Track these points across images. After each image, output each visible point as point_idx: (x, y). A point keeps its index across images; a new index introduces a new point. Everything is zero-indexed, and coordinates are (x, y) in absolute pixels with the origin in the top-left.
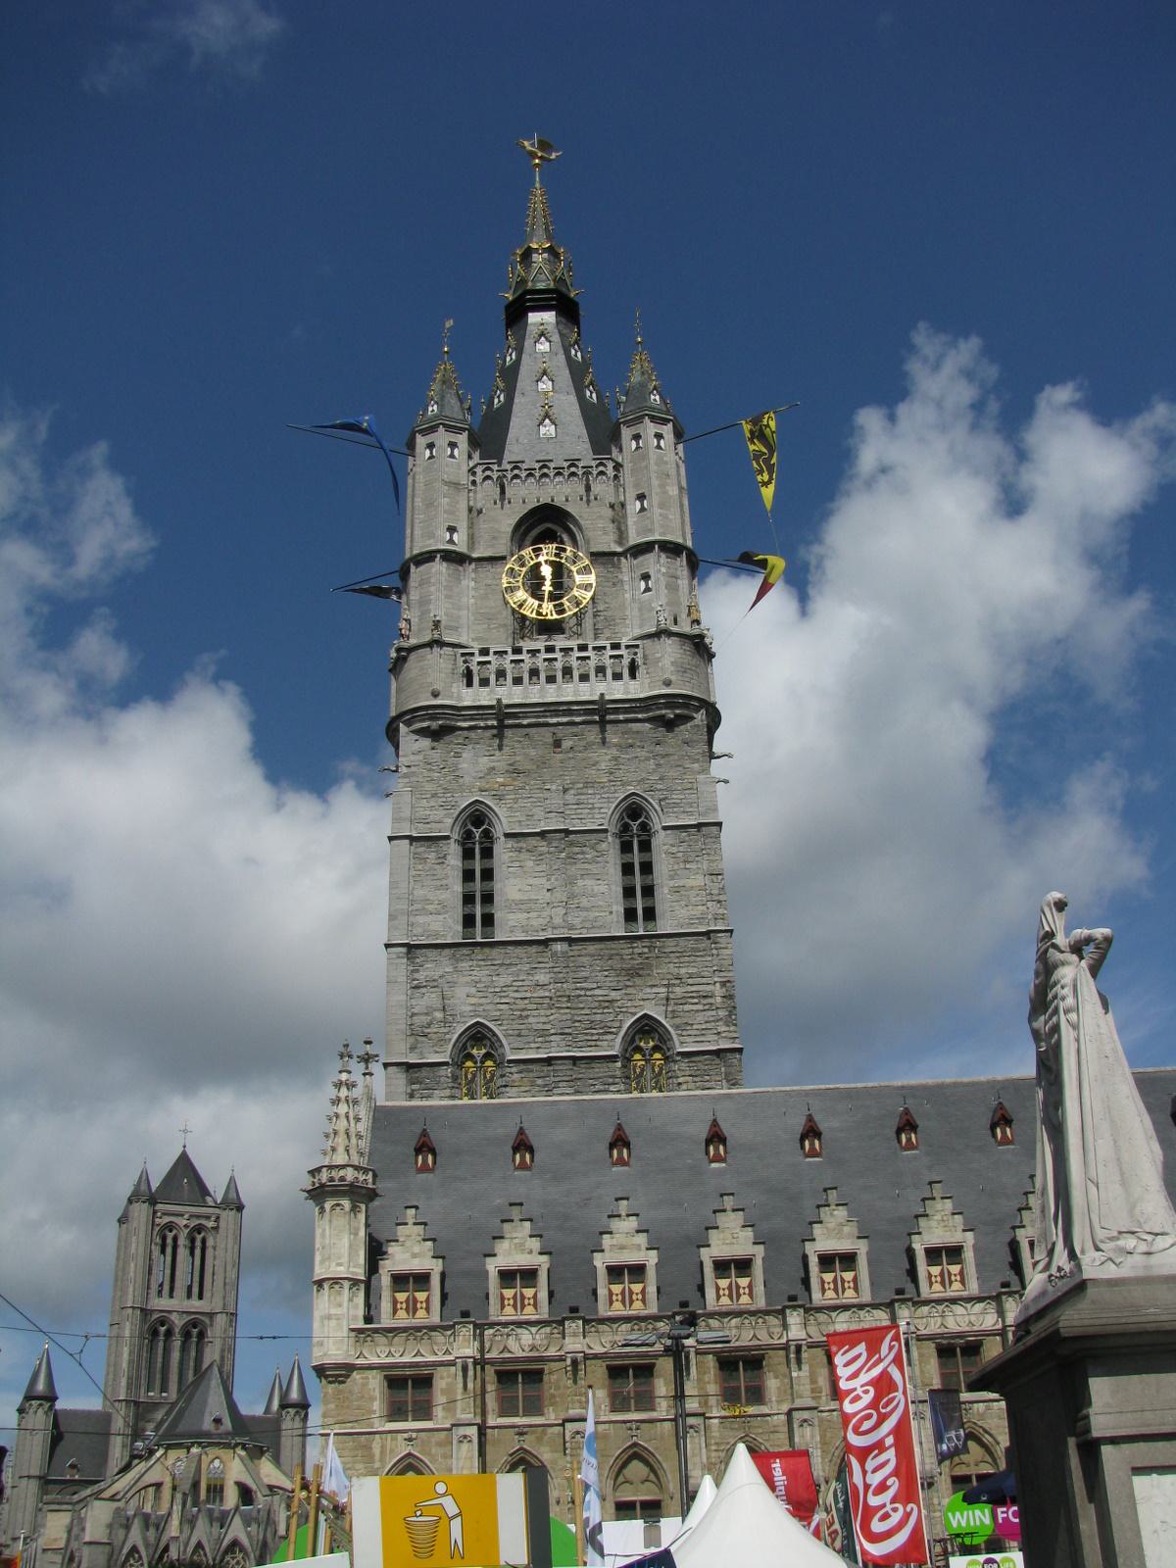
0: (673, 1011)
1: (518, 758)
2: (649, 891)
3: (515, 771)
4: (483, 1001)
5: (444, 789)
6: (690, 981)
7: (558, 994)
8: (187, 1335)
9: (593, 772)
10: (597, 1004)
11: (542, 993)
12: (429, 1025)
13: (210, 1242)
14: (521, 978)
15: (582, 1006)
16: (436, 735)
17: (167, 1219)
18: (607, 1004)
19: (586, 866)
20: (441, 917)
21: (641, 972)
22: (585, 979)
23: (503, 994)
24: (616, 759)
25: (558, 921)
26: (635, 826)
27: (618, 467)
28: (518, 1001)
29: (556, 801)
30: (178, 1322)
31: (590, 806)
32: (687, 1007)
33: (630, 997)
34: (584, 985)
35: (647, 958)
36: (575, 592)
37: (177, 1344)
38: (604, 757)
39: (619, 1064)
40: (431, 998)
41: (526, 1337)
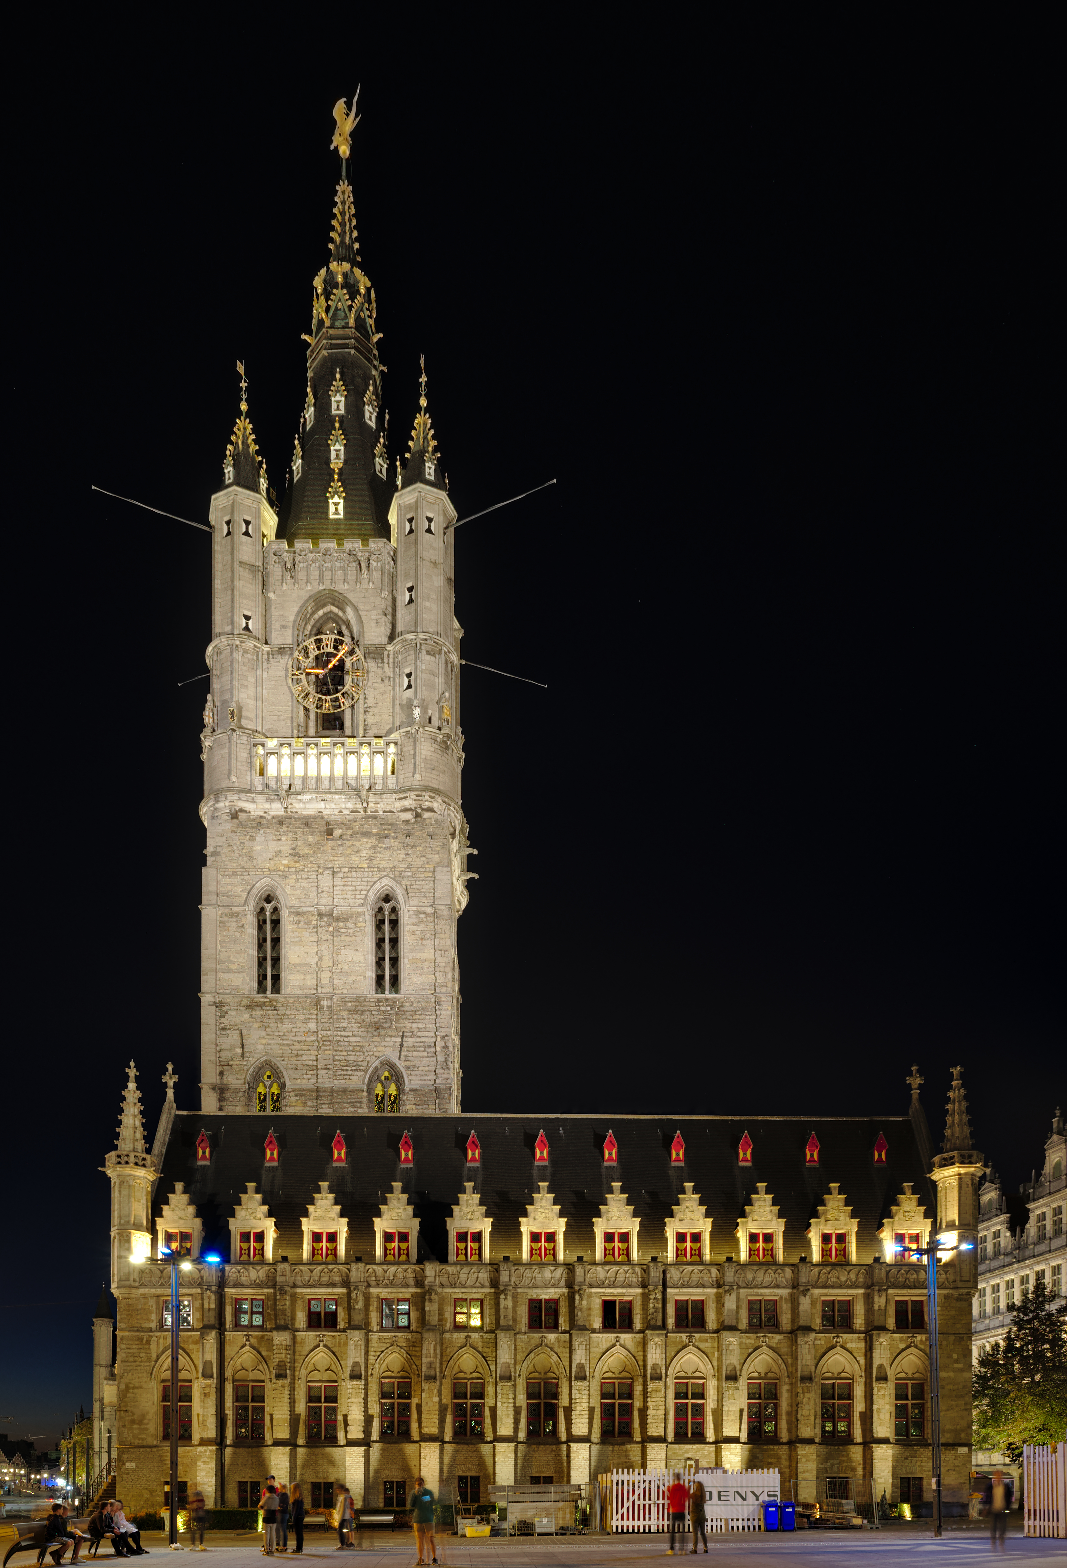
0: (406, 1056)
1: (299, 843)
3: (295, 855)
4: (270, 1042)
5: (243, 868)
6: (419, 1034)
7: (324, 1039)
9: (357, 859)
10: (351, 1048)
11: (313, 1038)
12: (232, 1059)
14: (298, 1025)
15: (340, 1049)
18: (358, 1049)
19: (348, 938)
20: (241, 975)
21: (384, 1025)
22: (345, 1029)
23: (284, 1038)
24: (374, 847)
28: (295, 1043)
31: (353, 888)
32: (415, 1054)
33: (376, 1044)
34: (343, 1033)
35: (390, 1014)
39: (365, 1094)
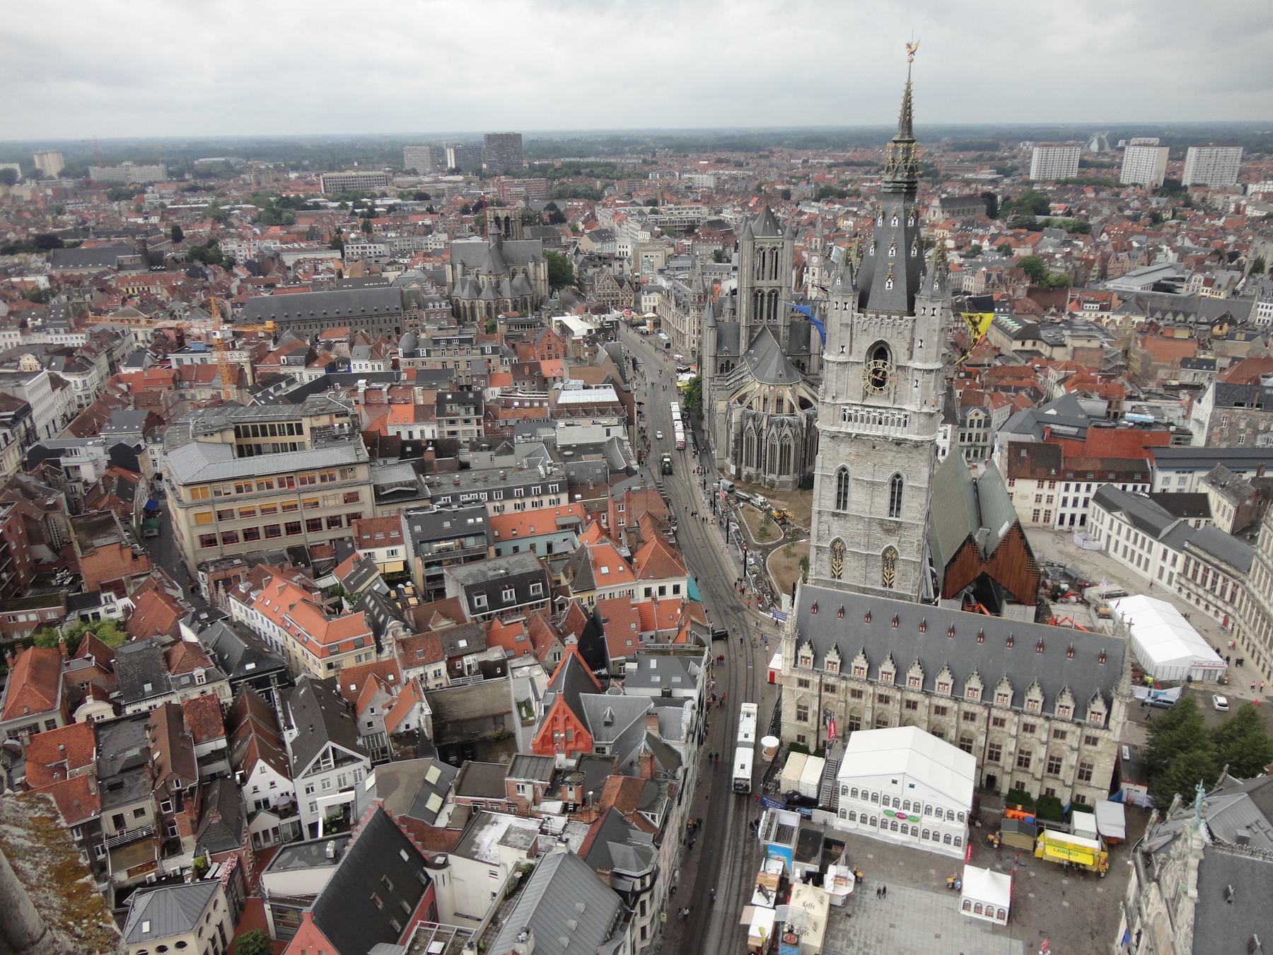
2: (899, 502)
3: (857, 455)
8: (770, 295)
13: (779, 254)
16: (833, 438)
17: (760, 246)
25: (867, 509)
26: (897, 480)
27: (914, 321)
29: (870, 470)
30: (766, 291)
36: (887, 384)
37: (766, 299)
38: (890, 455)
40: (825, 527)
41: (833, 679)
